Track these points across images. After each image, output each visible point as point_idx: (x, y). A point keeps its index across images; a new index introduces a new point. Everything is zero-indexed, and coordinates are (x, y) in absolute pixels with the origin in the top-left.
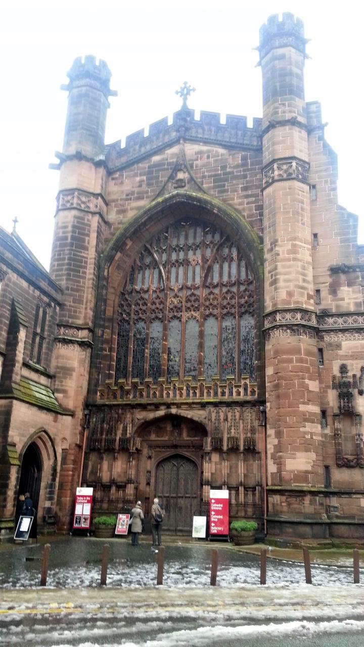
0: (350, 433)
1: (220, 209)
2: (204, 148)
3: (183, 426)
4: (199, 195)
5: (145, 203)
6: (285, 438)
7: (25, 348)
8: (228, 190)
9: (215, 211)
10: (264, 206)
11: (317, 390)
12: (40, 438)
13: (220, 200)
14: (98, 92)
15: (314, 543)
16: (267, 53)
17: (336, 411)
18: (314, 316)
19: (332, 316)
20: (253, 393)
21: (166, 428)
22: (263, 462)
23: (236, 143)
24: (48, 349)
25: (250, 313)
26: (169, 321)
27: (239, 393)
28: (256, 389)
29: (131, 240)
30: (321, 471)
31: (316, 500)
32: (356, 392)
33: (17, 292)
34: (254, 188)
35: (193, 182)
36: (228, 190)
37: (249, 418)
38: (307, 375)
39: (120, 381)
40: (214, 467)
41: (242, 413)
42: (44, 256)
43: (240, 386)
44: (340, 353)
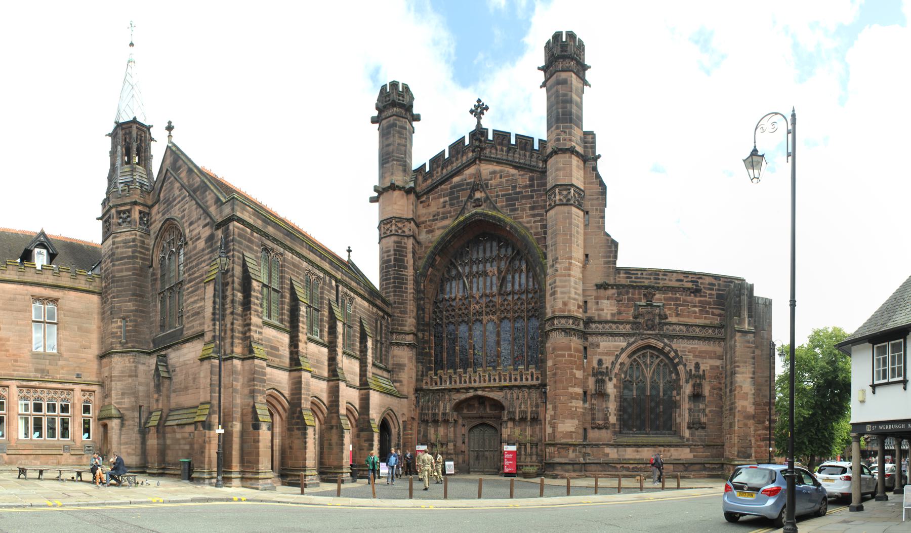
0: (602, 406)
1: (511, 227)
2: (498, 168)
3: (487, 403)
4: (494, 213)
5: (449, 223)
6: (559, 411)
7: (372, 353)
8: (518, 208)
9: (508, 229)
10: (548, 226)
11: (582, 377)
12: (388, 414)
13: (511, 217)
14: (404, 120)
15: (574, 474)
16: (551, 76)
17: (593, 392)
18: (581, 323)
19: (595, 322)
20: (537, 379)
21: (474, 405)
22: (543, 426)
23: (524, 164)
24: (386, 351)
25: (536, 317)
26: (473, 324)
27: (527, 380)
28: (540, 376)
29: (440, 256)
30: (581, 431)
31: (576, 450)
32: (608, 378)
33: (362, 311)
34: (540, 208)
35: (489, 201)
36: (518, 208)
37: (535, 397)
38: (575, 366)
39: (439, 372)
40: (509, 430)
41: (529, 393)
42: (373, 274)
43: (528, 374)
44: (599, 350)
